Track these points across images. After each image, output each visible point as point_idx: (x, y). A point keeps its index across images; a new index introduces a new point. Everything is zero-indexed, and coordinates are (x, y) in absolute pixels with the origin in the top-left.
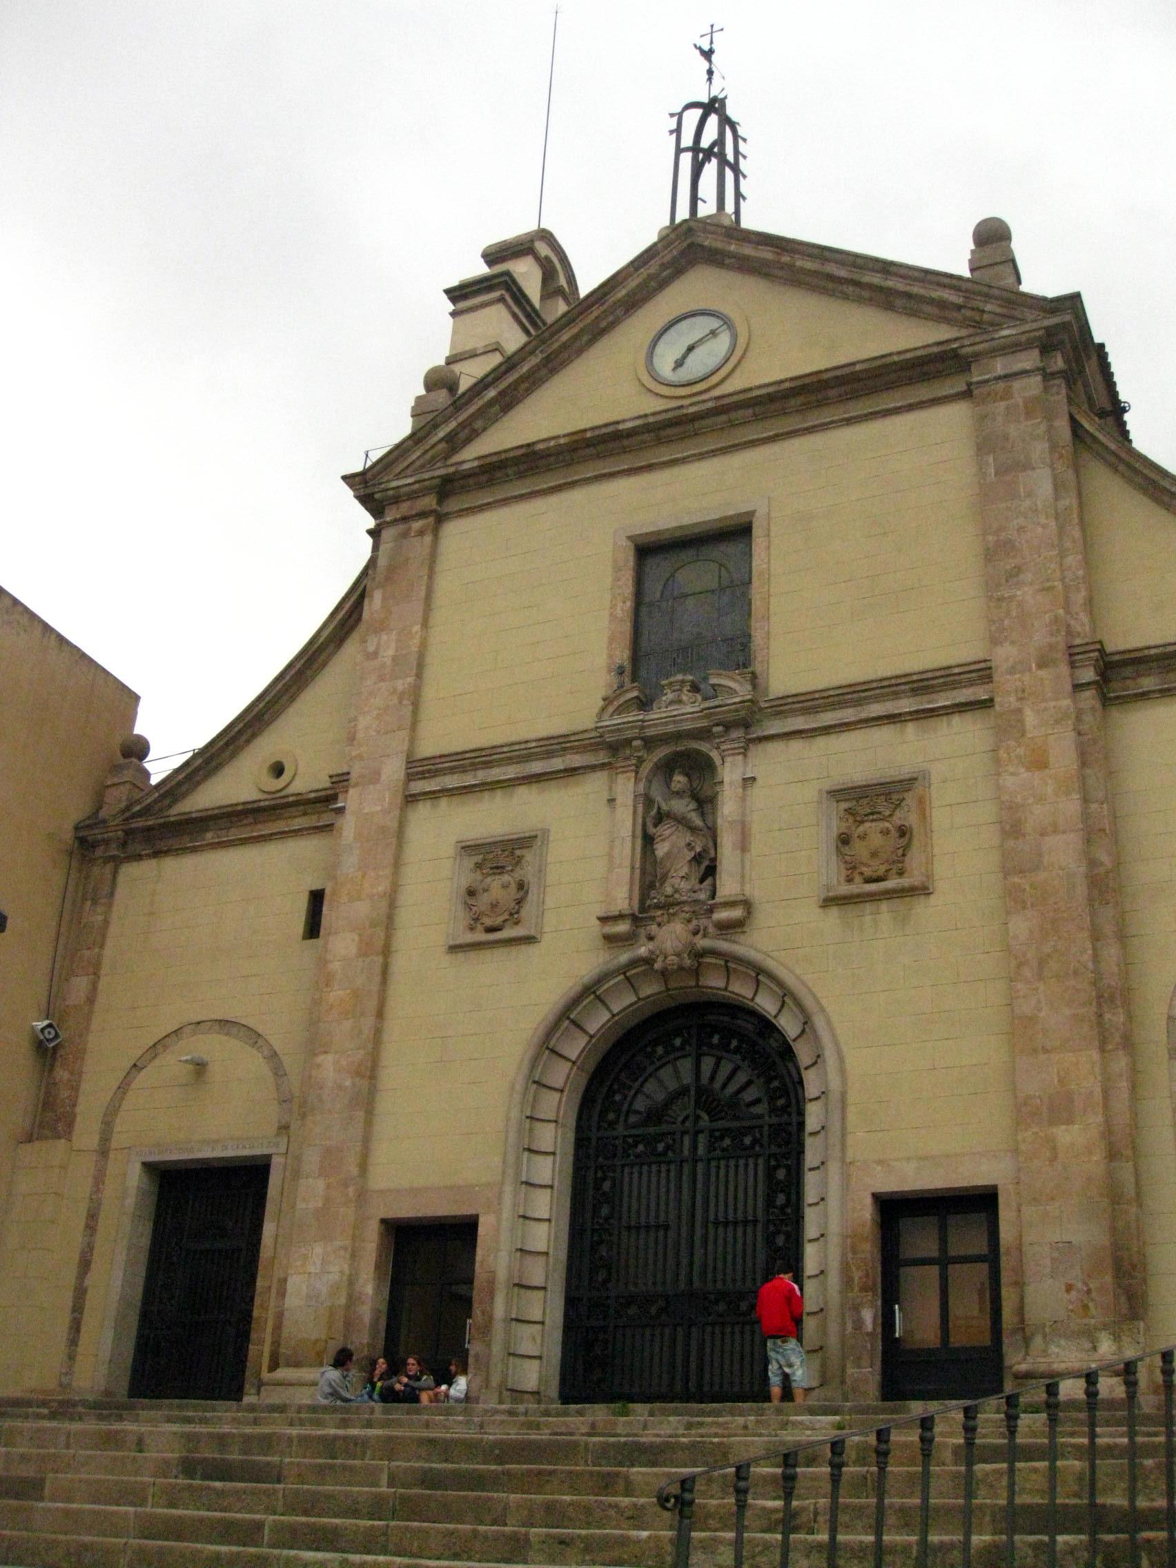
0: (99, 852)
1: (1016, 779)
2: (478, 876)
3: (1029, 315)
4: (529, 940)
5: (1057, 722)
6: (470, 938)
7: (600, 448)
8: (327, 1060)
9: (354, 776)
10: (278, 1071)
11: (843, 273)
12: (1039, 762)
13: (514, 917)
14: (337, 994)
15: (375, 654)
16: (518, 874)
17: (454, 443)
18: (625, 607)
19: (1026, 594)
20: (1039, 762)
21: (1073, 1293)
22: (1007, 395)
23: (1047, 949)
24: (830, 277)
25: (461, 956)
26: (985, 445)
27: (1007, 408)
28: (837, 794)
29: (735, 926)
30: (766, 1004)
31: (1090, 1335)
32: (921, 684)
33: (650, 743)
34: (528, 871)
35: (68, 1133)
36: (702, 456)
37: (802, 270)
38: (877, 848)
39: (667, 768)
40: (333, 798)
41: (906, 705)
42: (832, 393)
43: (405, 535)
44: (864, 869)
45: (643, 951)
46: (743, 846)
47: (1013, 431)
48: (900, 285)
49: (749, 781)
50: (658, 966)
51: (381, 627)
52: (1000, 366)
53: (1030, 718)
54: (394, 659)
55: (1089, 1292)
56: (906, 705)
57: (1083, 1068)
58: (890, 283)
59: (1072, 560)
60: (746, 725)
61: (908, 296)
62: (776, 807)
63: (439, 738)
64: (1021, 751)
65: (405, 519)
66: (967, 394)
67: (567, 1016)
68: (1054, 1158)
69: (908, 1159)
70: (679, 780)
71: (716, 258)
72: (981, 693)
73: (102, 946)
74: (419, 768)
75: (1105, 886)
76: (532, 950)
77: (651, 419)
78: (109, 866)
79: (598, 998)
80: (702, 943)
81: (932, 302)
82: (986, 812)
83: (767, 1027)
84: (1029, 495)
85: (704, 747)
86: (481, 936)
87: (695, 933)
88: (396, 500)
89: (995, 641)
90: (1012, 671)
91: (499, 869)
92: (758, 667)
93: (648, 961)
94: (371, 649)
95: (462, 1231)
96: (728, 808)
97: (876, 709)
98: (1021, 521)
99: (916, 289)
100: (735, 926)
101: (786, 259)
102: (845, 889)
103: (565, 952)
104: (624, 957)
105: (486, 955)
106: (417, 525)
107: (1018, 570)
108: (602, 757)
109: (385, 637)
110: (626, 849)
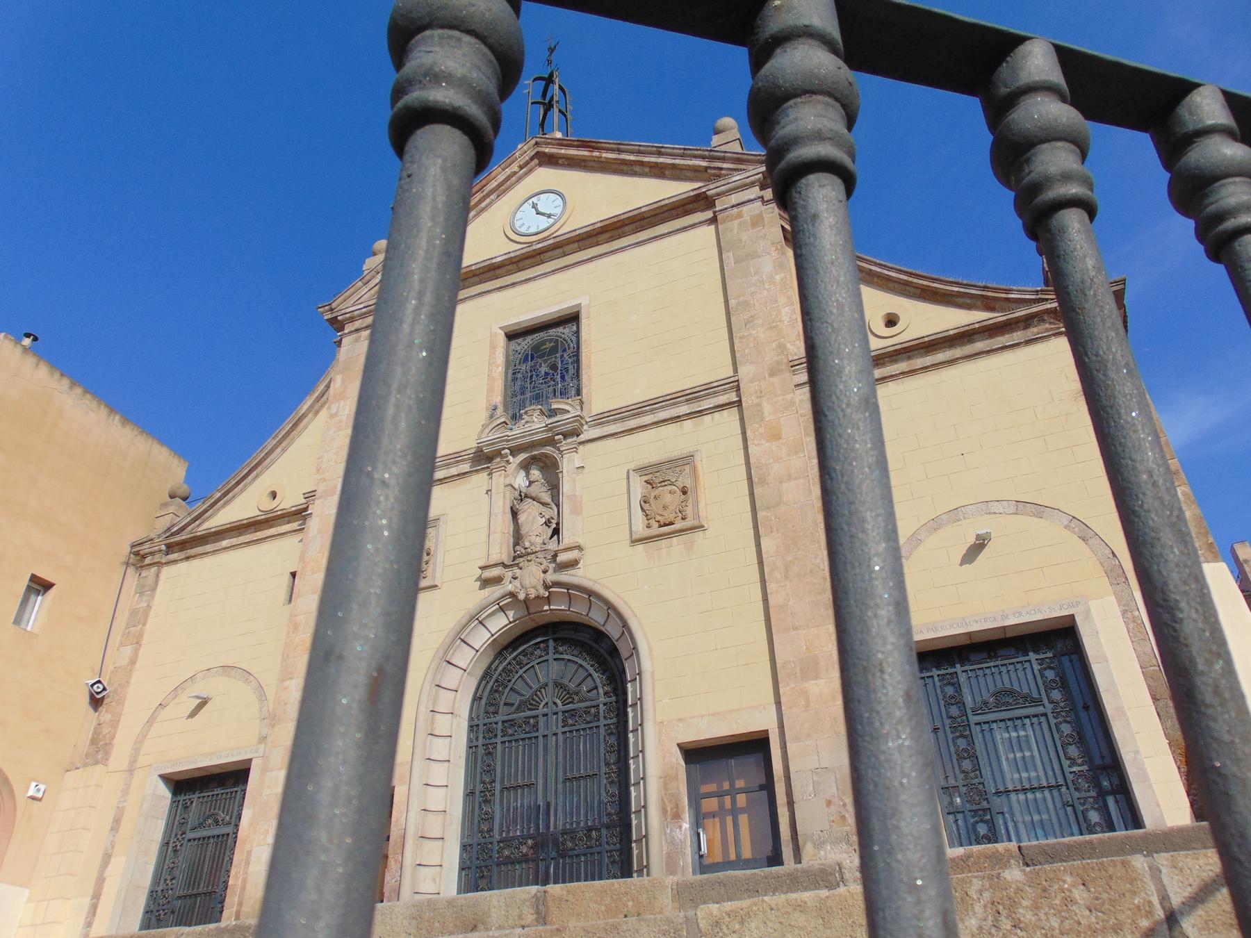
0: (148, 560)
4: (435, 587)
5: (786, 409)
7: (481, 277)
10: (262, 697)
11: (632, 158)
12: (775, 436)
15: (335, 415)
20: (775, 436)
21: (832, 807)
22: (739, 216)
23: (790, 558)
24: (624, 162)
27: (740, 224)
28: (641, 470)
29: (573, 564)
32: (692, 395)
35: (105, 761)
37: (608, 161)
40: (306, 509)
41: (684, 409)
42: (627, 228)
43: (357, 340)
44: (658, 518)
45: (510, 588)
46: (577, 511)
47: (745, 236)
48: (669, 161)
50: (522, 596)
55: (844, 805)
56: (684, 409)
58: (661, 160)
61: (674, 166)
62: (599, 481)
64: (762, 430)
65: (357, 330)
66: (713, 220)
68: (808, 706)
69: (702, 716)
73: (144, 624)
77: (512, 255)
78: (154, 569)
79: (480, 622)
80: (551, 577)
81: (689, 168)
83: (599, 635)
84: (756, 273)
85: (548, 450)
87: (545, 572)
88: (352, 320)
90: (752, 381)
92: (585, 398)
93: (512, 595)
94: (333, 411)
96: (566, 487)
98: (753, 289)
100: (573, 564)
101: (596, 154)
107: (753, 318)
109: (342, 403)
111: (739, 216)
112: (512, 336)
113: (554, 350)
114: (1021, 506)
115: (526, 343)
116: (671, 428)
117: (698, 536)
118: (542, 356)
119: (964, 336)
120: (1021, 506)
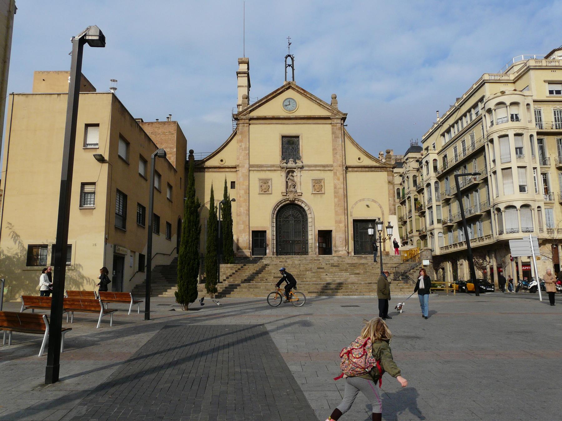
1: (336, 181)
8: (242, 208)
9: (240, 165)
12: (339, 180)
13: (268, 190)
14: (242, 199)
15: (241, 146)
17: (251, 111)
18: (281, 146)
19: (338, 156)
22: (336, 126)
26: (333, 133)
30: (303, 205)
32: (324, 166)
33: (287, 168)
34: (270, 184)
39: (288, 173)
51: (241, 141)
52: (336, 121)
54: (245, 148)
57: (343, 217)
59: (343, 152)
60: (301, 168)
63: (254, 161)
67: (277, 205)
70: (291, 174)
71: (293, 89)
72: (332, 169)
74: (250, 166)
75: (346, 196)
82: (332, 185)
86: (263, 192)
88: (242, 119)
89: (333, 162)
95: (264, 232)
97: (318, 168)
102: (314, 192)
104: (285, 198)
106: (246, 125)
107: (336, 153)
108: (279, 169)
110: (285, 183)
111: (336, 126)
112: (283, 137)
113: (293, 143)
119: (372, 167)
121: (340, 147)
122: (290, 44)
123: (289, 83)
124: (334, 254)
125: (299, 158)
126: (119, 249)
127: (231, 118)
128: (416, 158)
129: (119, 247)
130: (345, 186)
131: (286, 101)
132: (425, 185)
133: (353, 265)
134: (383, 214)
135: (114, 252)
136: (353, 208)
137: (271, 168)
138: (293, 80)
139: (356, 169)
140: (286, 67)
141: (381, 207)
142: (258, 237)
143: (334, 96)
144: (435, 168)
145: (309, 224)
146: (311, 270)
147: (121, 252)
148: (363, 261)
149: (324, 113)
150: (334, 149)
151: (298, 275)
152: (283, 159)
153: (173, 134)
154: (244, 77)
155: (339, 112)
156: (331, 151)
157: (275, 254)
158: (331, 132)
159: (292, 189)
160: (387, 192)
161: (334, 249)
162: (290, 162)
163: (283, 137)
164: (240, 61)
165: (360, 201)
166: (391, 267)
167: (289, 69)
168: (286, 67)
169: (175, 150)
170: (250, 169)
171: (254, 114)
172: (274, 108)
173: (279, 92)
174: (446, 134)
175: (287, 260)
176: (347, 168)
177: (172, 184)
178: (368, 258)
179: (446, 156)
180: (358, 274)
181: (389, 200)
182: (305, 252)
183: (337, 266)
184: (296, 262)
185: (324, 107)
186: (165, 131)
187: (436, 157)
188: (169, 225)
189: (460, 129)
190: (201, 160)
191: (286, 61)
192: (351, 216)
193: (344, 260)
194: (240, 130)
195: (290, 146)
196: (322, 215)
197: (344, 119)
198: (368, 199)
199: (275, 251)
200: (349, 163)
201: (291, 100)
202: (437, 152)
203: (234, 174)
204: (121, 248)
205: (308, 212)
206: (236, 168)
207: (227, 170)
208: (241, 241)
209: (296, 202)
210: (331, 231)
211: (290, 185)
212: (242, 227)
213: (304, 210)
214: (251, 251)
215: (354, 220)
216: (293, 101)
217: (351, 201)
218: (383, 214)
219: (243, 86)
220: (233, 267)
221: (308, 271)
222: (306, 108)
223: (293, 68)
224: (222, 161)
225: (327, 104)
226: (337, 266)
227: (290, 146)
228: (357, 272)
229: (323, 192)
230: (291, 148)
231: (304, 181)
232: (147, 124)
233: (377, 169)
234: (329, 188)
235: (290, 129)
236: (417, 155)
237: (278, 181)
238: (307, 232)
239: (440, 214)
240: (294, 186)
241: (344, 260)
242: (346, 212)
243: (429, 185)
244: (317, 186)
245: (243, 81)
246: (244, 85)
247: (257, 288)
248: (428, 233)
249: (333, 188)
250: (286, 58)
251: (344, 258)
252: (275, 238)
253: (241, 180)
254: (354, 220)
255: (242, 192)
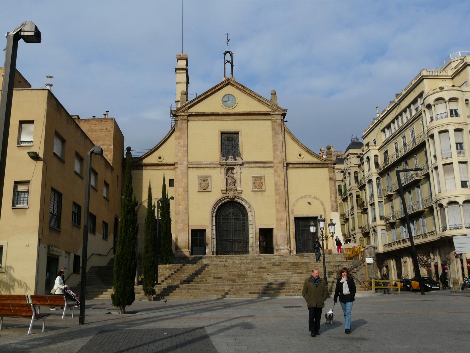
1: (277, 178)
2: (201, 181)
3: (280, 111)
6: (200, 190)
8: (180, 207)
9: (179, 163)
11: (253, 95)
12: (279, 176)
13: (207, 188)
14: (180, 197)
15: (179, 143)
16: (207, 182)
17: (190, 107)
18: (220, 143)
22: (276, 122)
25: (199, 193)
26: (273, 129)
28: (253, 177)
30: (243, 203)
31: (284, 245)
32: (264, 163)
33: (227, 165)
34: (209, 181)
36: (231, 120)
38: (258, 183)
41: (262, 165)
43: (182, 122)
45: (227, 195)
47: (277, 128)
49: (241, 173)
51: (180, 138)
52: (275, 117)
53: (278, 170)
54: (184, 145)
56: (262, 165)
57: (284, 215)
58: (260, 99)
59: (284, 148)
60: (240, 165)
66: (271, 120)
67: (217, 203)
70: (230, 171)
71: (233, 85)
72: (272, 165)
74: (189, 163)
75: (287, 193)
76: (211, 193)
80: (236, 195)
82: (273, 182)
86: (202, 190)
88: (180, 116)
89: (274, 159)
91: (204, 181)
97: (258, 165)
99: (264, 101)
102: (254, 190)
103: (216, 194)
104: (225, 195)
105: (203, 193)
106: (184, 121)
107: (277, 149)
108: (219, 166)
110: (224, 181)
111: (276, 122)
112: (222, 133)
114: (315, 198)
115: (225, 136)
116: (259, 168)
117: (264, 192)
118: (230, 141)
119: (313, 164)
120: (315, 198)
121: (280, 144)
122: (228, 41)
123: (228, 79)
124: (275, 253)
125: (239, 155)
126: (53, 250)
127: (169, 115)
128: (357, 154)
129: (53, 248)
130: (286, 183)
131: (225, 97)
132: (367, 182)
133: (295, 264)
134: (325, 211)
135: (48, 253)
136: (294, 205)
137: (211, 165)
138: (232, 76)
139: (296, 166)
140: (225, 64)
141: (322, 204)
142: (198, 236)
143: (273, 92)
144: (377, 164)
145: (250, 223)
146: (252, 269)
147: (55, 253)
148: (305, 260)
149: (264, 109)
150: (274, 146)
151: (238, 275)
152: (223, 156)
153: (110, 131)
154: (182, 73)
155: (279, 108)
156: (272, 147)
157: (215, 253)
158: (271, 128)
159: (232, 186)
160: (329, 189)
161: (275, 247)
162: (230, 159)
163: (222, 133)
164: (179, 57)
165: (302, 198)
166: (334, 266)
167: (228, 65)
168: (225, 64)
169: (112, 147)
170: (189, 166)
171: (193, 110)
172: (213, 104)
173: (218, 88)
174: (386, 130)
175: (228, 260)
176: (287, 164)
177: (109, 181)
178: (311, 256)
179: (386, 152)
180: (301, 273)
181: (331, 197)
182: (245, 251)
183: (278, 265)
184: (237, 262)
185: (263, 103)
186: (102, 128)
187: (377, 152)
188: (105, 225)
189: (401, 125)
190: (139, 158)
191: (225, 57)
192: (293, 213)
193: (285, 259)
194: (178, 126)
195: (230, 143)
196: (262, 213)
197: (284, 115)
198: (310, 196)
199: (215, 250)
200: (290, 160)
201: (230, 96)
202: (378, 147)
203: (172, 172)
204: (55, 249)
205: (248, 210)
206: (174, 165)
207: (166, 167)
208: (179, 240)
209: (236, 200)
210: (272, 229)
211: (230, 182)
212: (180, 225)
213: (244, 208)
214: (190, 250)
215: (295, 218)
216: (232, 97)
217: (292, 198)
218: (325, 211)
219: (181, 83)
220: (171, 268)
221: (249, 270)
222: (245, 104)
223: (232, 64)
224: (160, 158)
225: (266, 100)
226: (278, 265)
227: (230, 143)
228: (300, 271)
229: (263, 189)
230: (230, 144)
231: (244, 177)
232: (83, 121)
233: (318, 165)
234: (269, 184)
235: (230, 126)
236: (358, 151)
237: (218, 178)
238: (248, 230)
239: (383, 210)
240: (234, 183)
241: (285, 259)
242: (287, 209)
243: (370, 181)
244: (258, 183)
245: (182, 77)
246: (183, 81)
247: (196, 289)
248: (371, 230)
249: (273, 185)
250: (225, 54)
251: (286, 257)
252: (214, 237)
253: (180, 177)
254: (295, 218)
255: (181, 190)
